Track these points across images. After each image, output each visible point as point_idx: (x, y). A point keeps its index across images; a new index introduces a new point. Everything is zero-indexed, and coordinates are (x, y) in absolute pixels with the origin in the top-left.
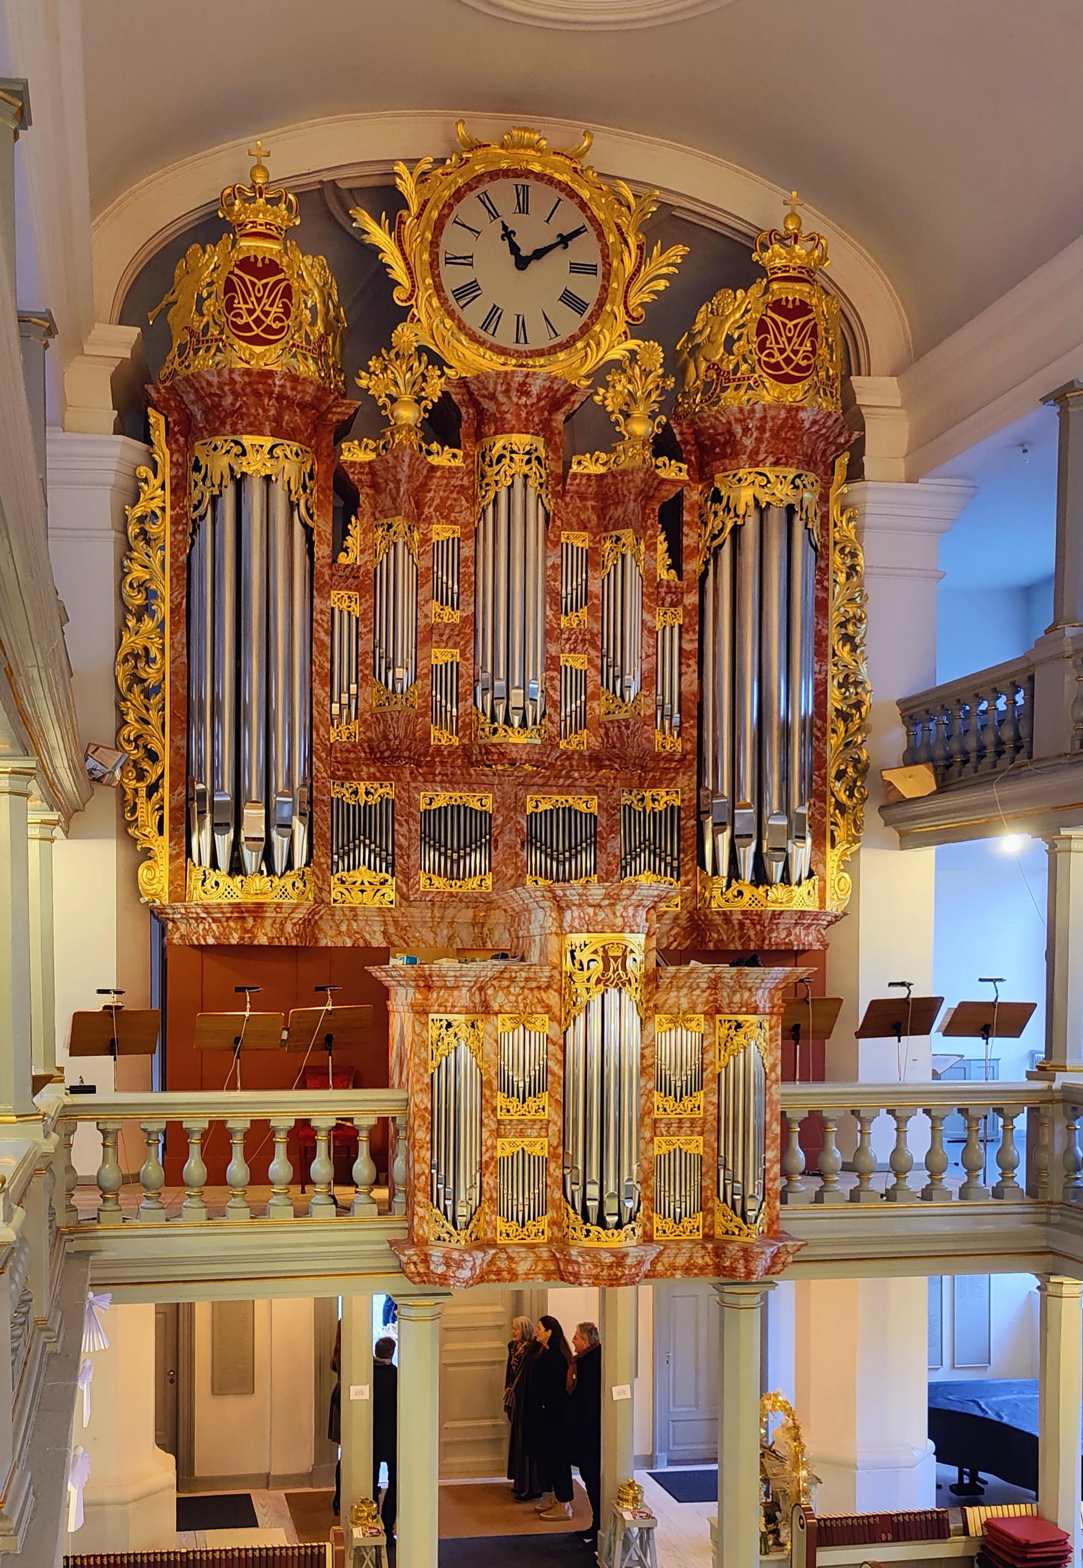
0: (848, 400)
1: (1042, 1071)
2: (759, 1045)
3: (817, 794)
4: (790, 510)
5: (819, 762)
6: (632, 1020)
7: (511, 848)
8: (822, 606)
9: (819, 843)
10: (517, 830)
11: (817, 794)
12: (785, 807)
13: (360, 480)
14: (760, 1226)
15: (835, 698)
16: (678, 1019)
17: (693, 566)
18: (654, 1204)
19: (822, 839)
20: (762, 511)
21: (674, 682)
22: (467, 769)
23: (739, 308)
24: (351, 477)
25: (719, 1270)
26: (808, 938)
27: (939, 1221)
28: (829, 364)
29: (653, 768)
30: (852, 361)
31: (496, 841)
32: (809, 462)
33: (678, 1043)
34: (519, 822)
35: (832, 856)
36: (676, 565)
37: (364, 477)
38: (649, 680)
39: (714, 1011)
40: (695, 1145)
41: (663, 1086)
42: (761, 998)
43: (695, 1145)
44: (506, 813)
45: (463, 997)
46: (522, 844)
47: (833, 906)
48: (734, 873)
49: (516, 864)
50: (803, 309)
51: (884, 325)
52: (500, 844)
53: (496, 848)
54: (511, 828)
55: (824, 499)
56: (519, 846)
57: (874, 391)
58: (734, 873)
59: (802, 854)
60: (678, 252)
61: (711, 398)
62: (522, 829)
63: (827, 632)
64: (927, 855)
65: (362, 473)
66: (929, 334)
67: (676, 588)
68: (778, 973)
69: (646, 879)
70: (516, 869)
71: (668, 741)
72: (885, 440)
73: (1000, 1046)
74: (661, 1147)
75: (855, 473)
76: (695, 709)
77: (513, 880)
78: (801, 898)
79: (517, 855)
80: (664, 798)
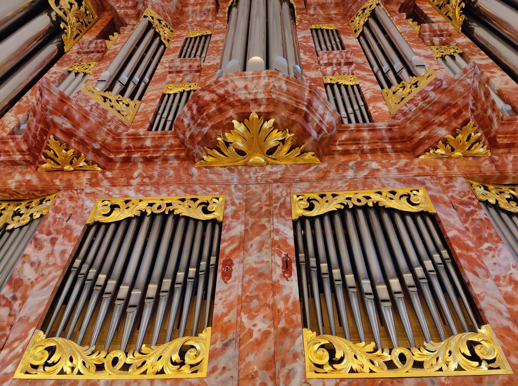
7: (261, 275)
10: (274, 243)
13: (127, 15)
22: (186, 169)
24: (118, 11)
31: (229, 263)
34: (277, 231)
37: (130, 12)
44: (251, 221)
46: (286, 265)
49: (273, 307)
52: (237, 270)
53: (227, 275)
54: (262, 244)
56: (279, 271)
62: (284, 241)
65: (127, 8)
67: (441, 31)
70: (275, 317)
77: (270, 344)
79: (275, 288)
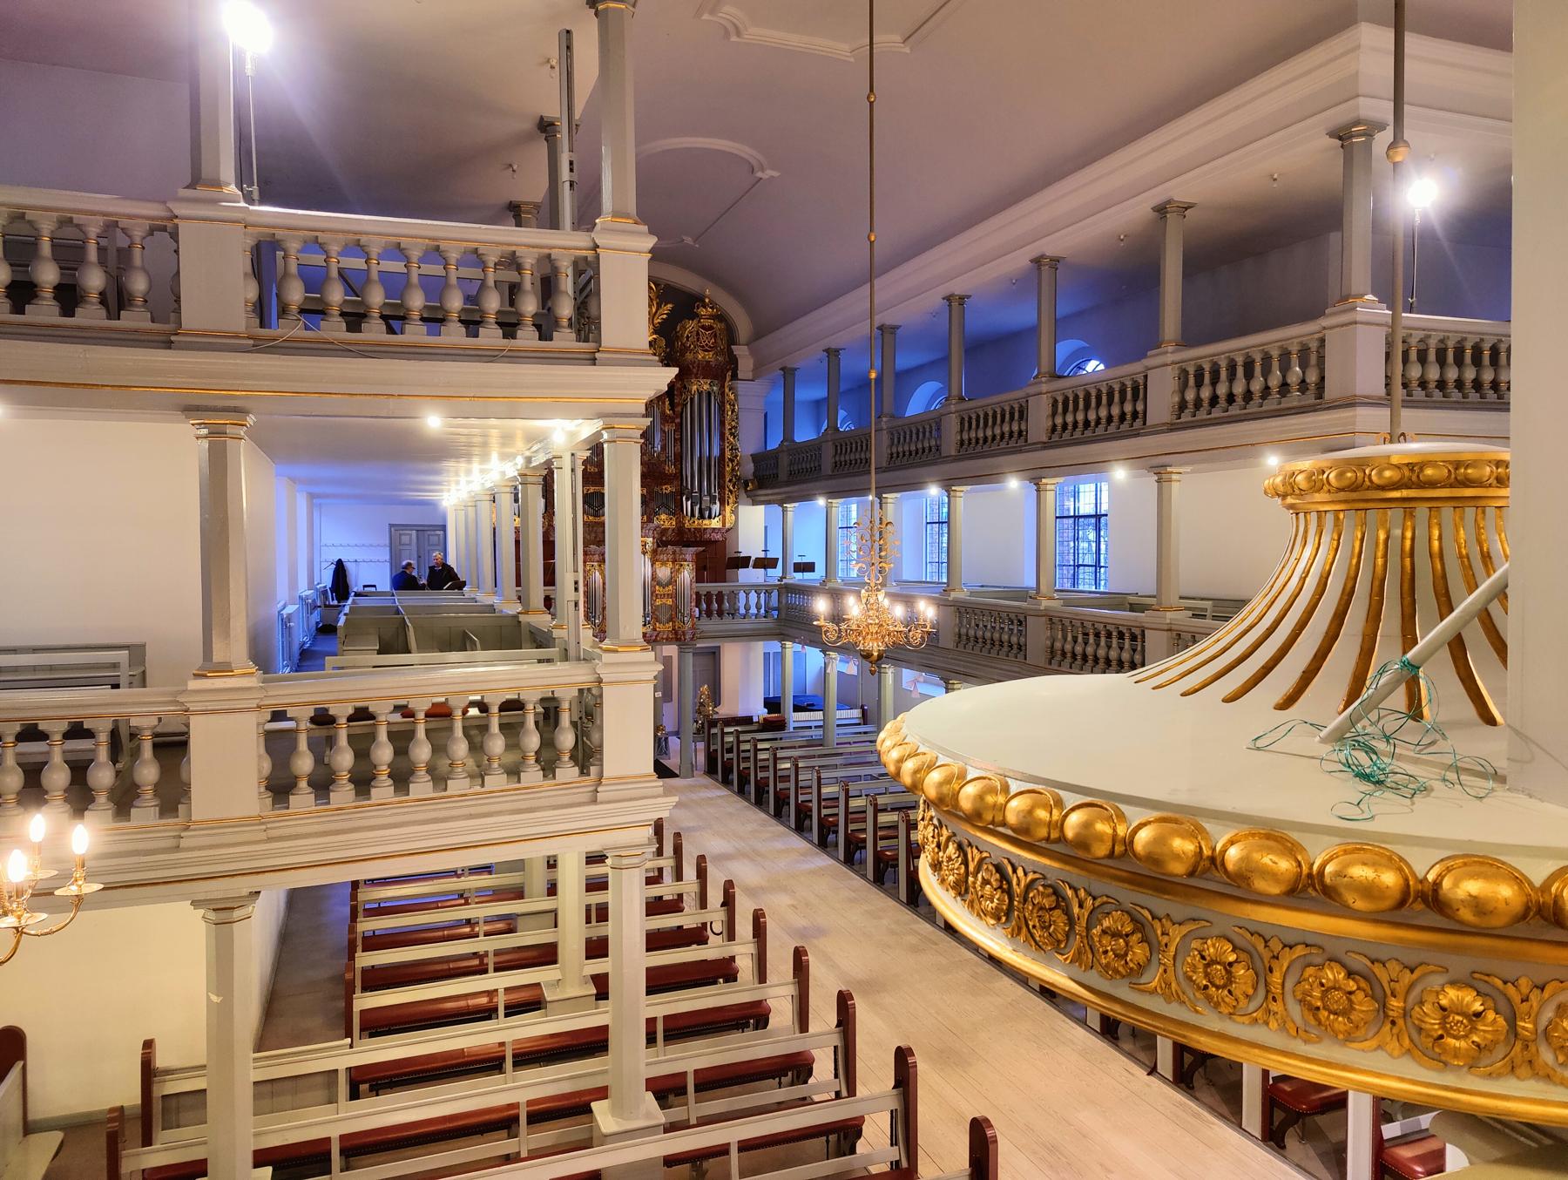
0: (730, 352)
1: (781, 579)
2: (687, 575)
3: (722, 487)
4: (709, 394)
5: (721, 475)
6: (649, 564)
8: (722, 423)
9: (722, 503)
11: (722, 487)
12: (709, 493)
14: (690, 624)
15: (728, 454)
16: (664, 563)
17: (678, 409)
18: (657, 620)
19: (722, 503)
20: (700, 394)
21: (671, 451)
23: (691, 325)
25: (678, 640)
26: (718, 537)
27: (746, 625)
28: (722, 345)
29: (667, 479)
30: (732, 339)
32: (714, 377)
33: (664, 572)
35: (728, 509)
36: (672, 409)
38: (664, 448)
39: (674, 561)
40: (670, 602)
41: (659, 584)
42: (688, 557)
43: (670, 602)
45: (596, 557)
47: (728, 526)
48: (693, 515)
50: (710, 328)
51: (743, 327)
55: (723, 386)
57: (740, 351)
58: (693, 515)
59: (716, 508)
60: (669, 306)
61: (683, 355)
63: (727, 431)
64: (762, 508)
66: (758, 334)
68: (693, 549)
69: (663, 517)
71: (672, 469)
72: (745, 365)
73: (770, 571)
74: (658, 602)
75: (735, 377)
76: (679, 458)
78: (715, 523)
80: (668, 489)
